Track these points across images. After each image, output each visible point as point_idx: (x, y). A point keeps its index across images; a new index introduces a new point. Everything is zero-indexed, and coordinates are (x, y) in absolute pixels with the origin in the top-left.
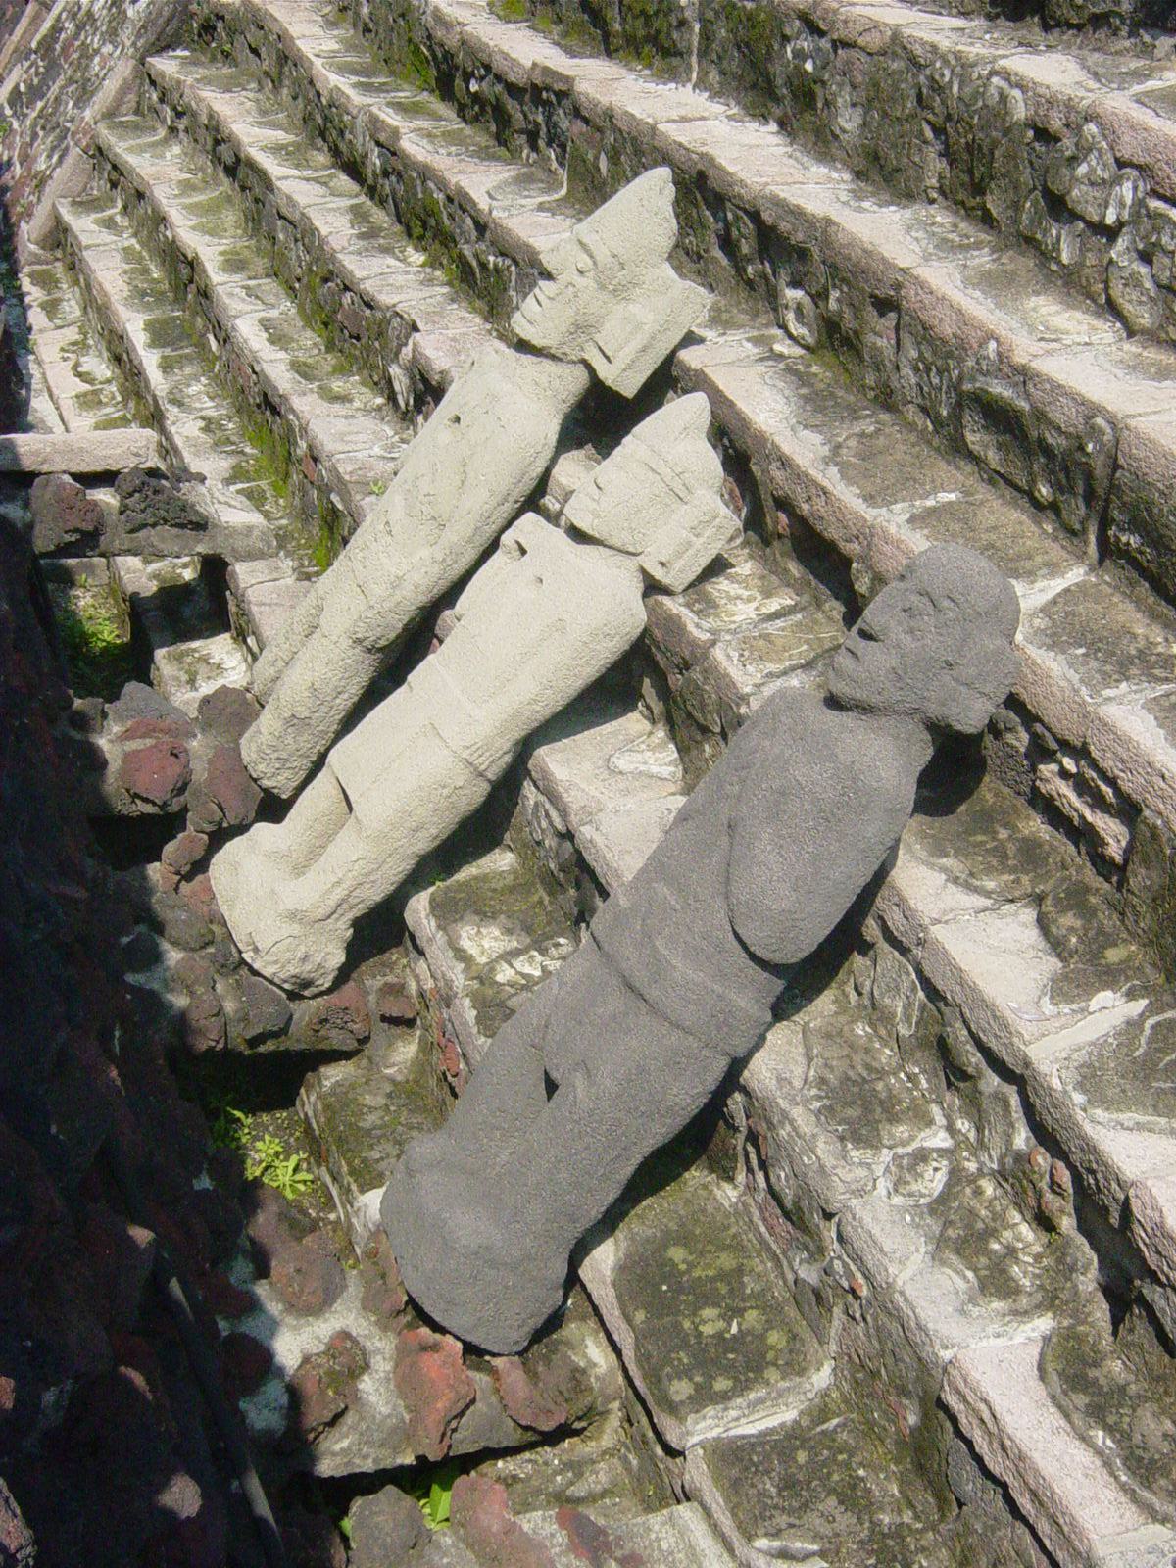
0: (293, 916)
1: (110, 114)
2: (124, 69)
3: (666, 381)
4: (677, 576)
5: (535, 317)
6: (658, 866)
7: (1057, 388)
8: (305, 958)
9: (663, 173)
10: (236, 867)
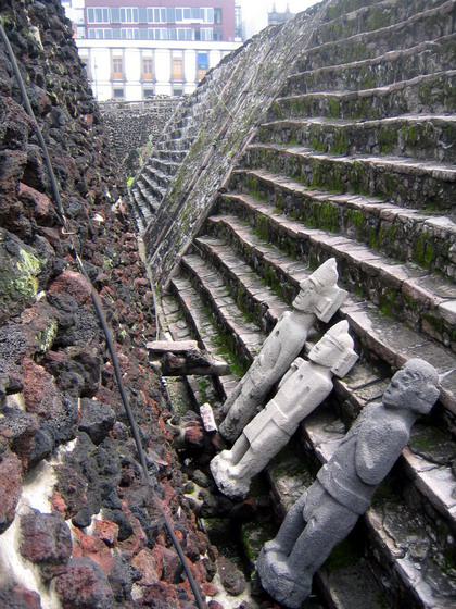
0: (233, 477)
1: (186, 254)
2: (189, 241)
3: (338, 317)
4: (341, 374)
5: (298, 302)
6: (335, 458)
7: (447, 311)
8: (237, 490)
9: (333, 259)
10: (217, 464)
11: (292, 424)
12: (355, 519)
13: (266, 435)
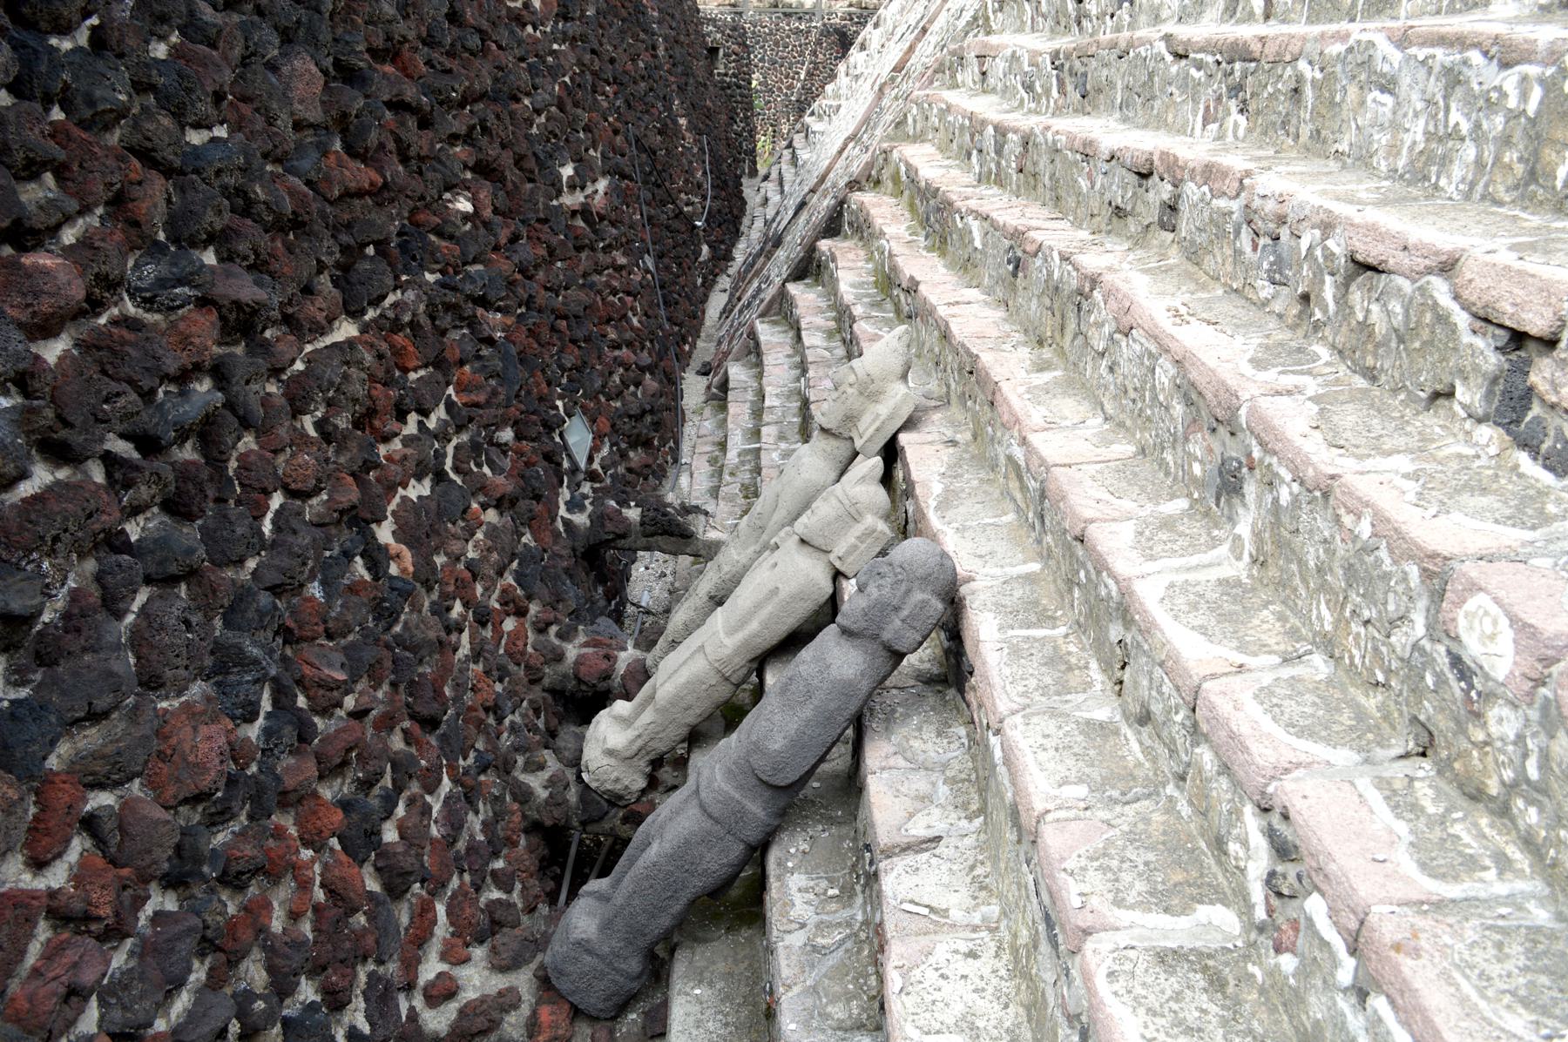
0: (610, 753)
8: (617, 780)
11: (737, 660)
12: (736, 851)
13: (683, 676)
